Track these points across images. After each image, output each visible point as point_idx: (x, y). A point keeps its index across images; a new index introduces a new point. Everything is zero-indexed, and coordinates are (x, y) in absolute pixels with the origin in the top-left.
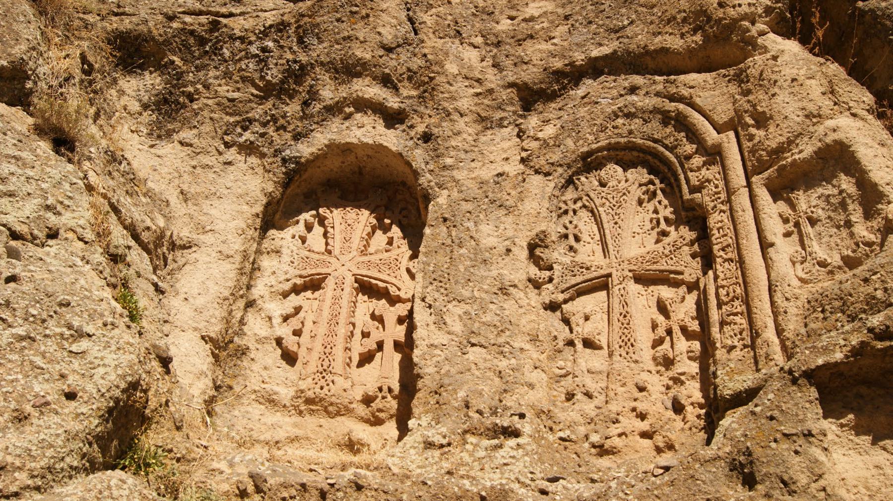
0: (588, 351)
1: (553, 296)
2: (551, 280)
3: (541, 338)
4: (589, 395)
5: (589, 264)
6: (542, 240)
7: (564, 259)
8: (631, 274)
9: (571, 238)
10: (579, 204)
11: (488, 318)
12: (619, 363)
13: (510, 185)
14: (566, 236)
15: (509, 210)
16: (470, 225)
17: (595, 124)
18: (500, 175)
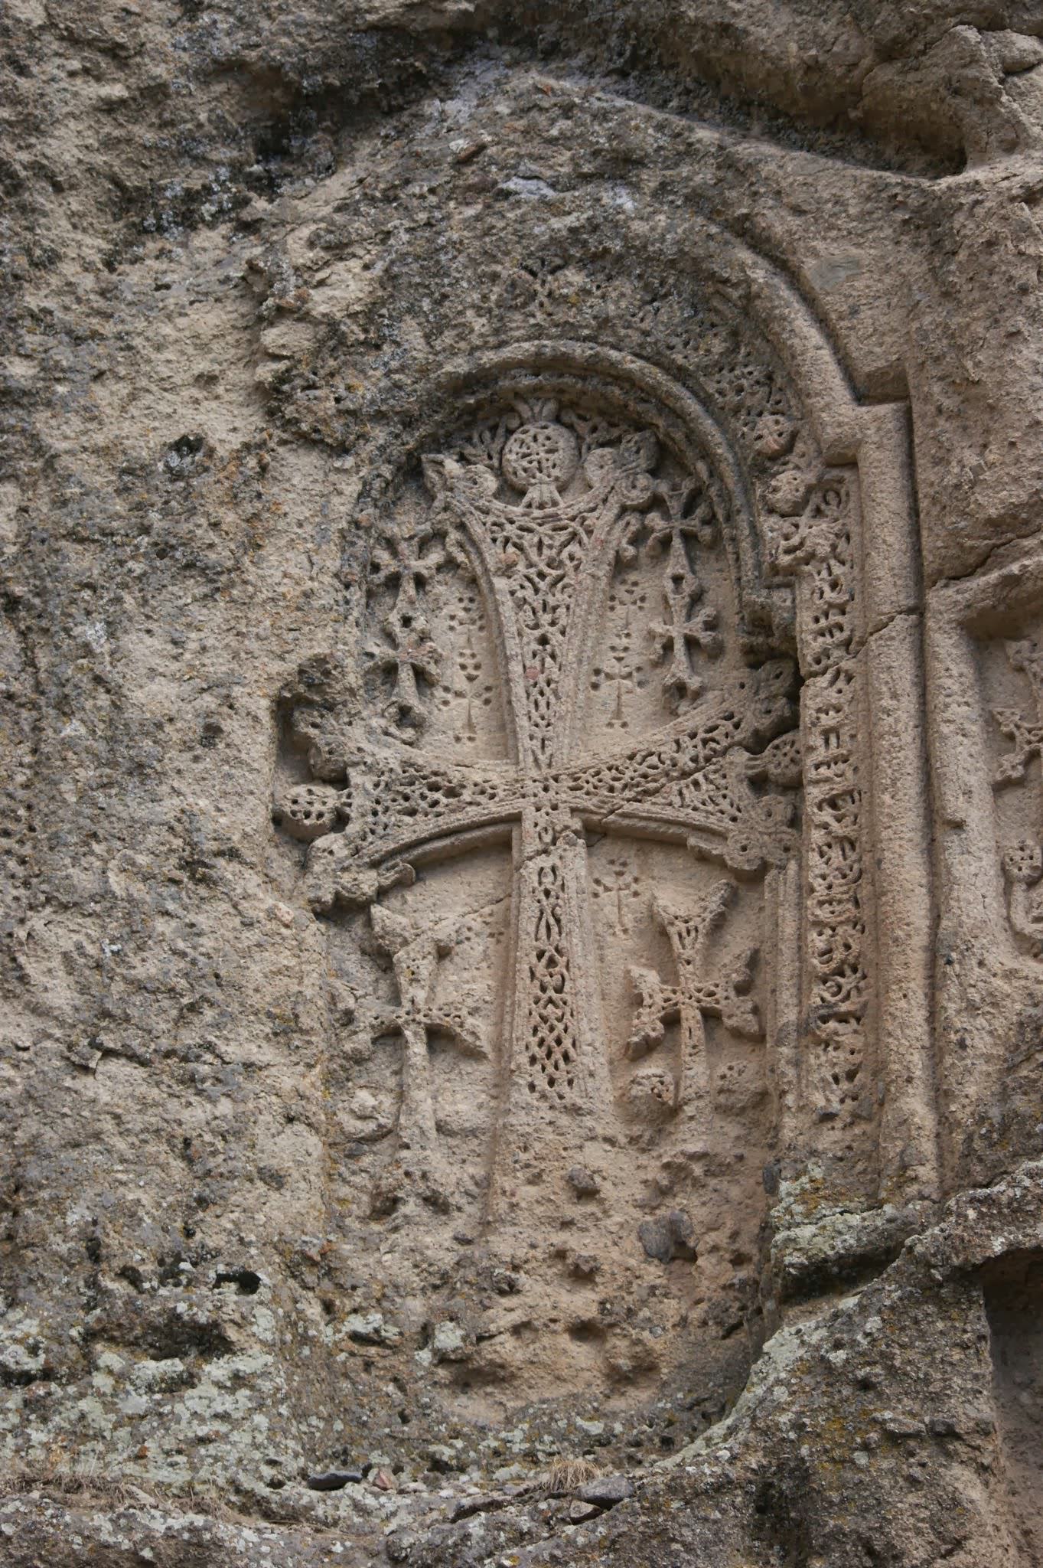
0: (443, 1061)
1: (346, 878)
2: (341, 820)
3: (305, 1022)
4: (436, 1204)
5: (456, 776)
6: (318, 687)
7: (383, 753)
8: (576, 824)
9: (406, 676)
10: (435, 557)
11: (146, 968)
12: (528, 1114)
13: (219, 491)
14: (390, 671)
15: (216, 582)
16: (92, 632)
17: (495, 277)
18: (188, 445)
